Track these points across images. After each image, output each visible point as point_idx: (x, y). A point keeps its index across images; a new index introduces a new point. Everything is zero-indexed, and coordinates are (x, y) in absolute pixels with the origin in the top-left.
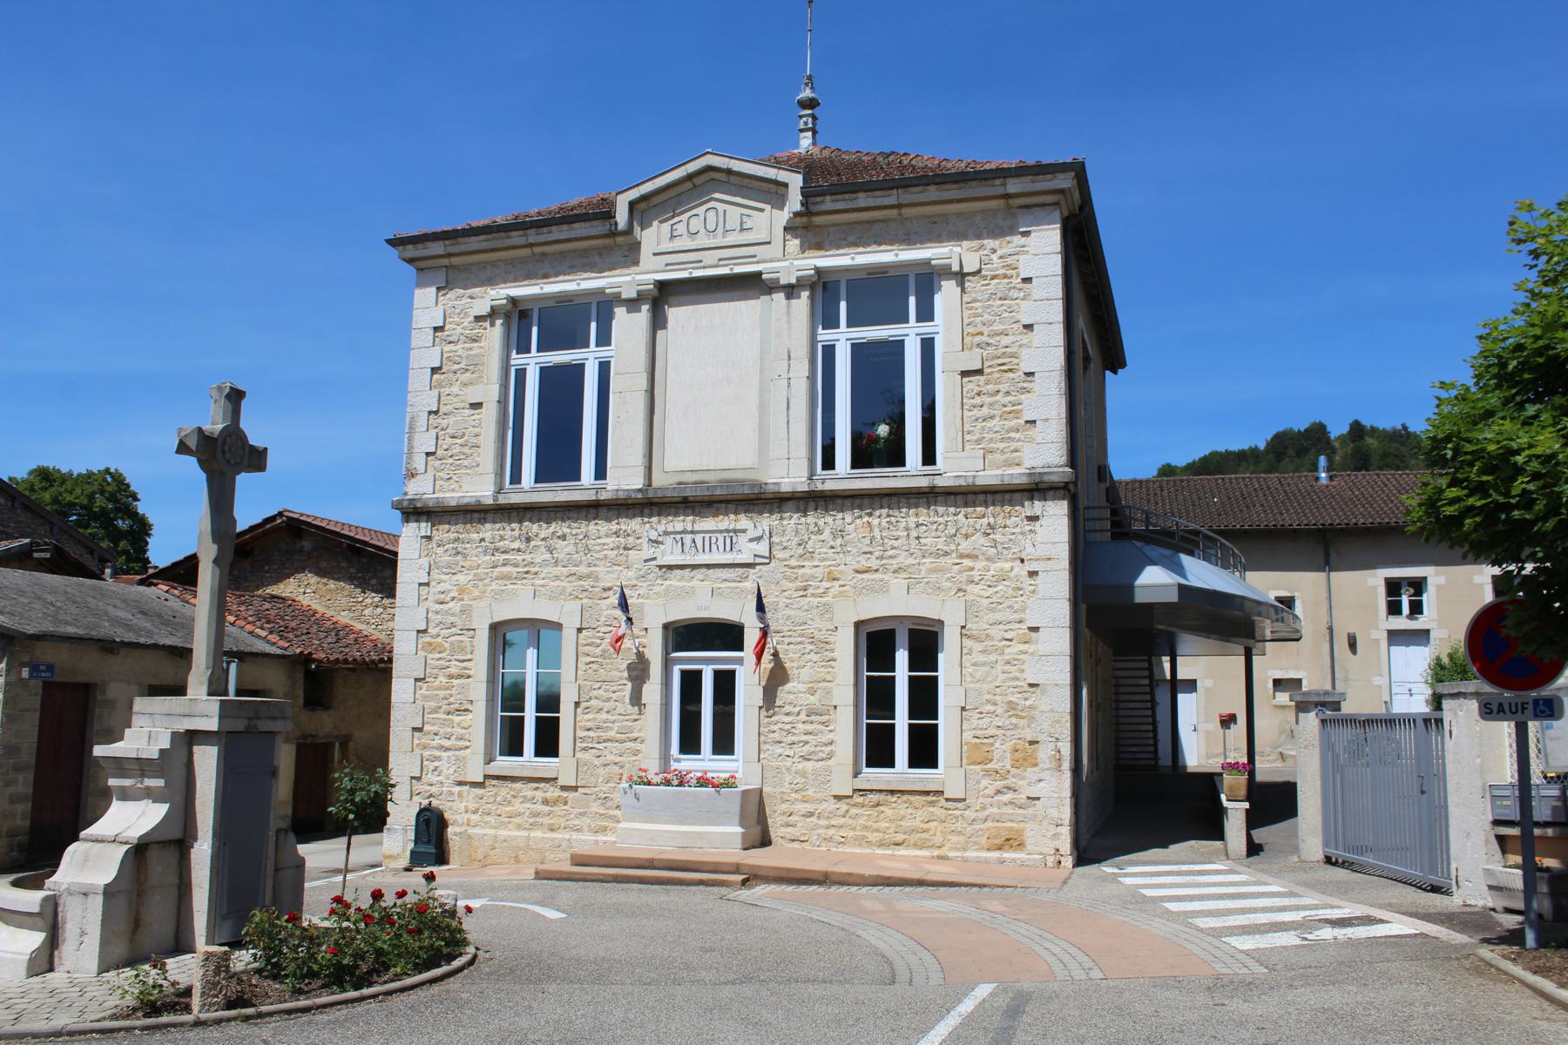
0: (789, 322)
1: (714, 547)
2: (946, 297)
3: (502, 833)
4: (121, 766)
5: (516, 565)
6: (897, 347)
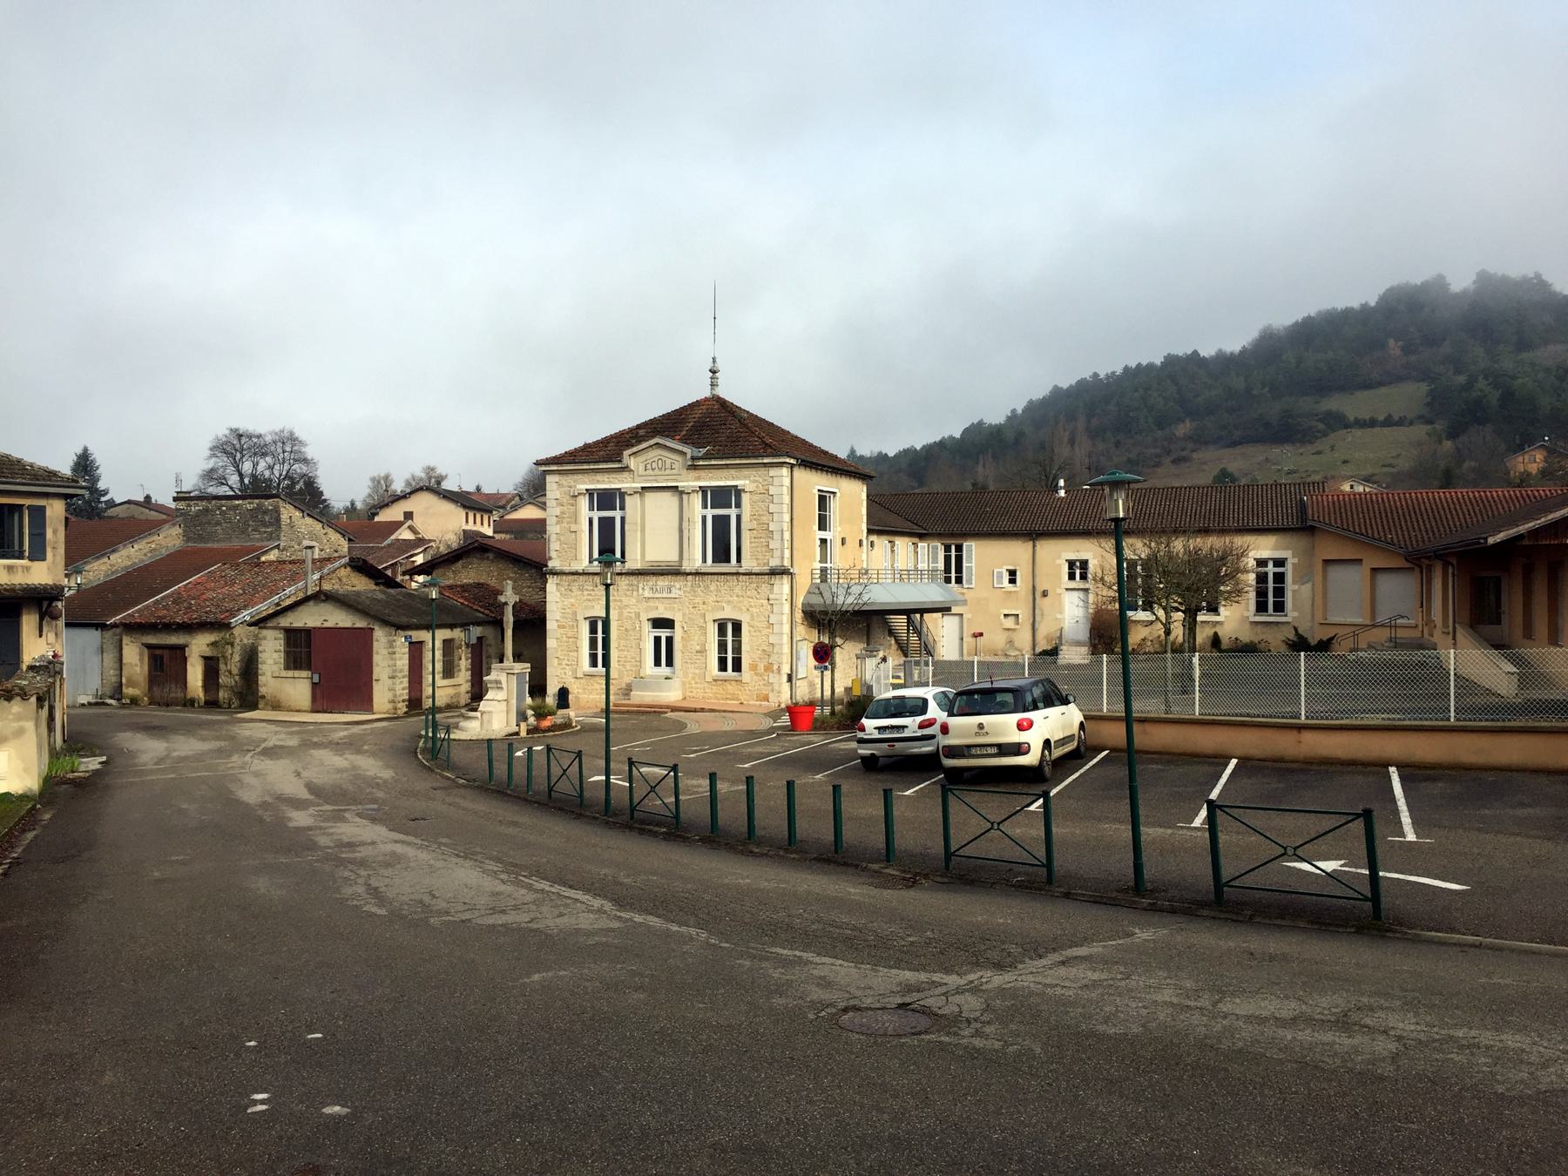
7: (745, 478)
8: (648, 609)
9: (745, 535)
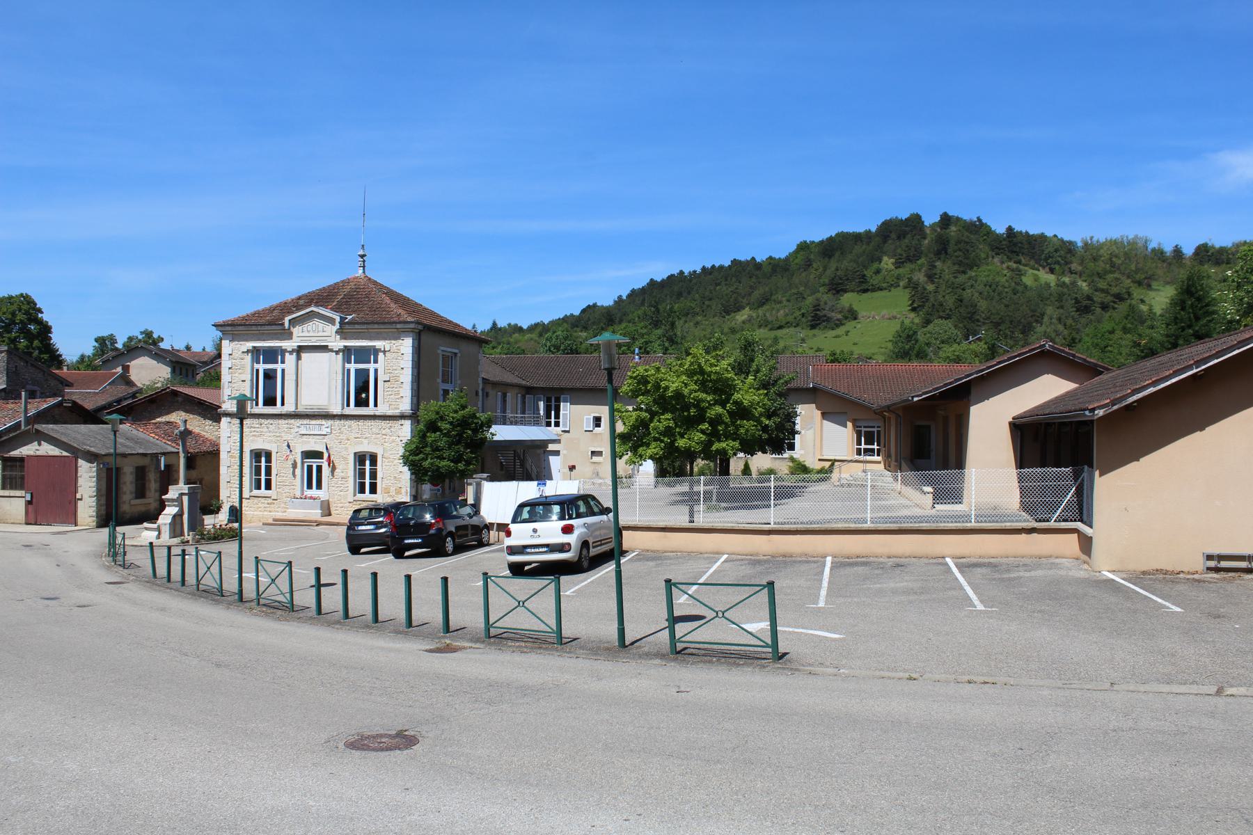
4: (168, 500)
6: (368, 371)
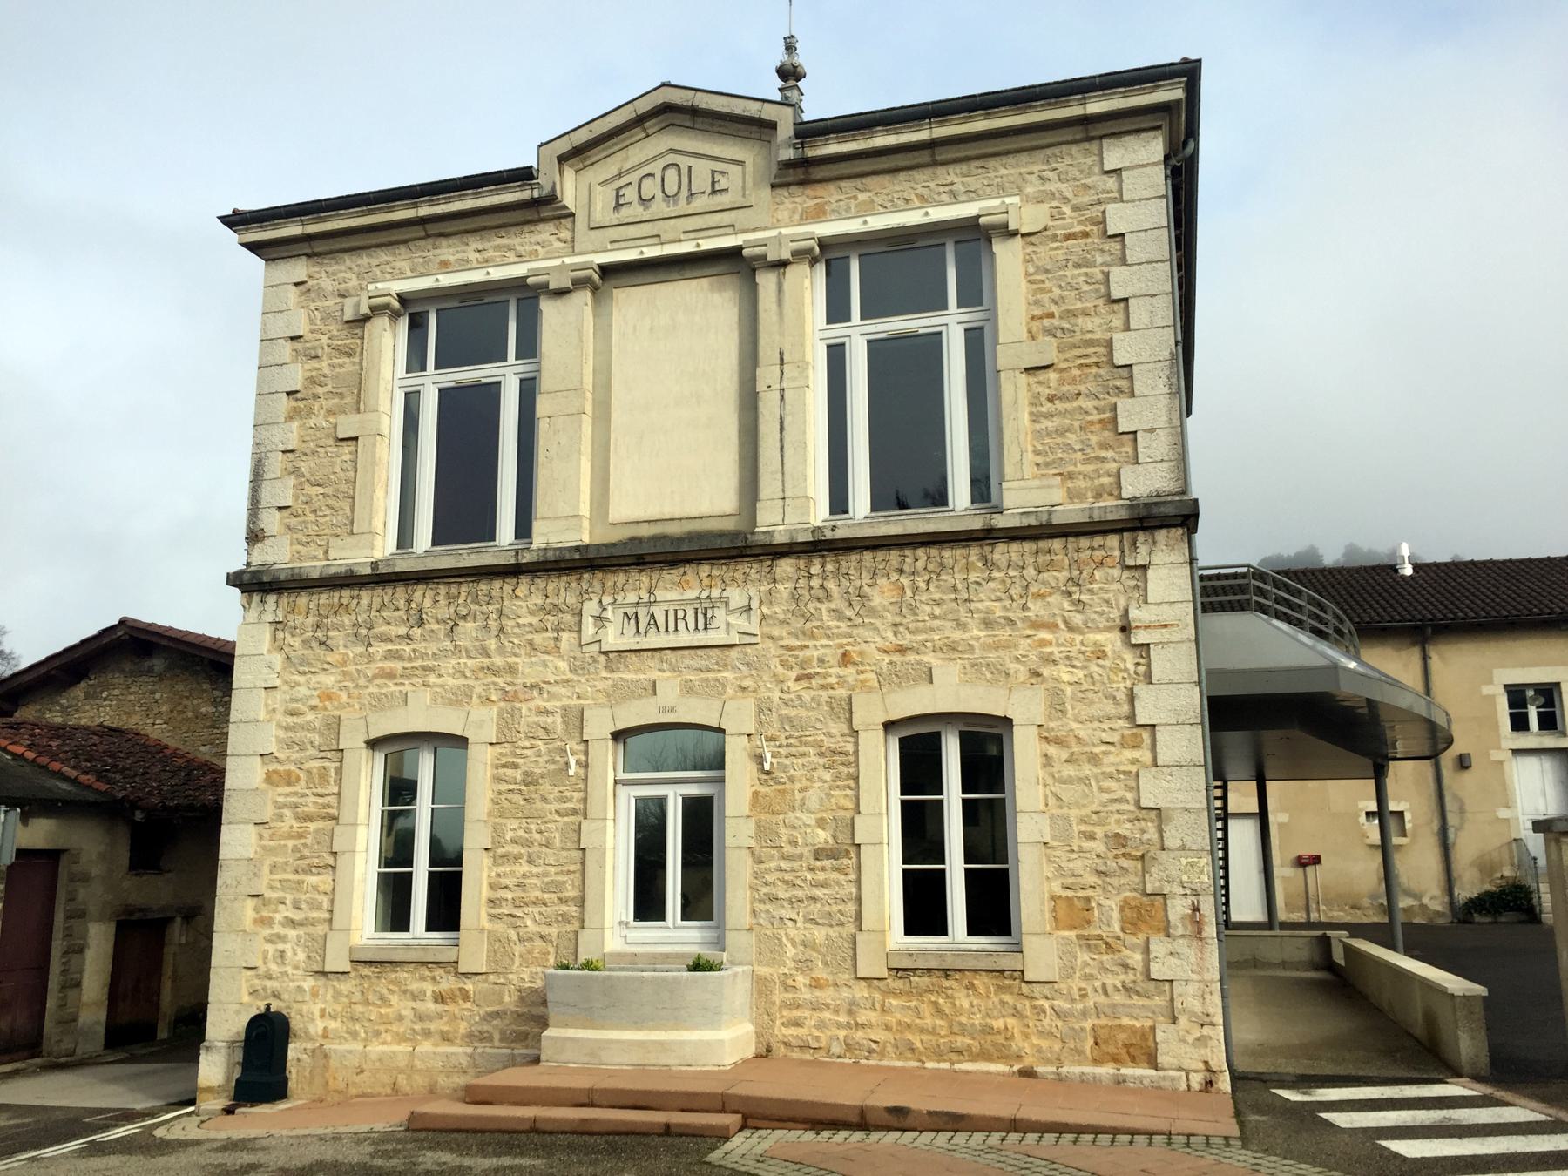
0: (781, 314)
1: (681, 625)
2: (1008, 259)
3: (376, 1048)
5: (401, 658)
6: (933, 343)
7: (1002, 190)
8: (619, 695)
9: (1015, 399)
